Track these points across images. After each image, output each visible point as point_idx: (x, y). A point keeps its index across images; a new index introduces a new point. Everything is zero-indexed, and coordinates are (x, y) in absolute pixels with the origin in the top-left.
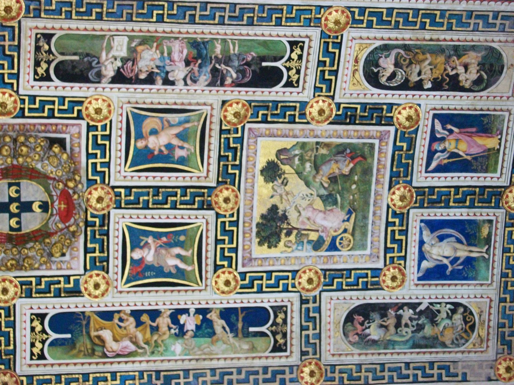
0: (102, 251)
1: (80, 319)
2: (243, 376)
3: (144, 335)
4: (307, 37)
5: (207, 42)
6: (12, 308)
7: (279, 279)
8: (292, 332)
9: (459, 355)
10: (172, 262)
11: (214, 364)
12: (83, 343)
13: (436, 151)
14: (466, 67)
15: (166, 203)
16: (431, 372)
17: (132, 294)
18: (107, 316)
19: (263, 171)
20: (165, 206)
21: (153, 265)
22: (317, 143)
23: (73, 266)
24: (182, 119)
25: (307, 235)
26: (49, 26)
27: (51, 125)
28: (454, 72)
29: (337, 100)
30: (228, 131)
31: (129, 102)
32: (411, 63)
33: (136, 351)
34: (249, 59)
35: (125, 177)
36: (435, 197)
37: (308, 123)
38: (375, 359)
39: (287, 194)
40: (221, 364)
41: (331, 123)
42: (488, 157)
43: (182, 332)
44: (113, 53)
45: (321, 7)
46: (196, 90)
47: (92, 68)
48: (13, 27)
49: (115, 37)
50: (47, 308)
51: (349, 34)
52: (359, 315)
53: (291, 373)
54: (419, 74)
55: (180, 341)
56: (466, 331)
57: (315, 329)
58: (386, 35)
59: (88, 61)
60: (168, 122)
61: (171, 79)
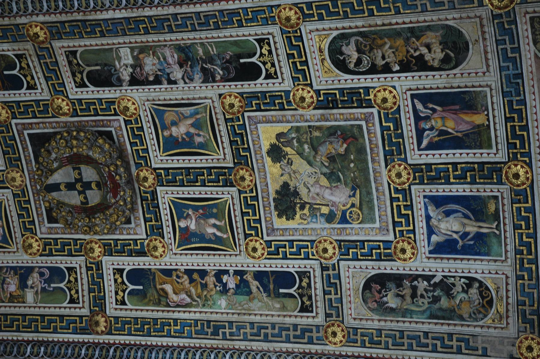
0: (157, 221)
1: (148, 274)
2: (276, 331)
3: (196, 290)
4: (269, 34)
5: (190, 46)
6: (100, 263)
7: (300, 248)
8: (316, 295)
9: (478, 330)
10: (211, 230)
11: (253, 318)
12: (152, 294)
13: (424, 130)
14: (428, 47)
15: (197, 182)
16: (450, 343)
17: (184, 256)
18: (168, 273)
19: (268, 153)
20: (197, 184)
21: (196, 233)
22: (309, 127)
23: (138, 232)
24: (192, 111)
25: (319, 209)
26: (71, 44)
27: (99, 121)
28: (417, 53)
29: (315, 87)
30: (232, 120)
31: (148, 100)
32: (371, 49)
33: (191, 303)
34: (228, 57)
35: (162, 160)
36: (433, 174)
37: (296, 109)
38: (394, 326)
39: (294, 172)
40: (258, 319)
41: (315, 108)
42: (479, 134)
43: (225, 290)
44: (123, 62)
45: (272, 7)
46: (195, 87)
47: (112, 75)
48: (48, 48)
49: (120, 49)
50: (123, 264)
51: (306, 28)
52: (376, 283)
53: (318, 332)
54: (383, 58)
55: (224, 297)
56: (483, 306)
57: (336, 294)
58: (340, 25)
59: (108, 69)
60: (182, 114)
61: (173, 79)
